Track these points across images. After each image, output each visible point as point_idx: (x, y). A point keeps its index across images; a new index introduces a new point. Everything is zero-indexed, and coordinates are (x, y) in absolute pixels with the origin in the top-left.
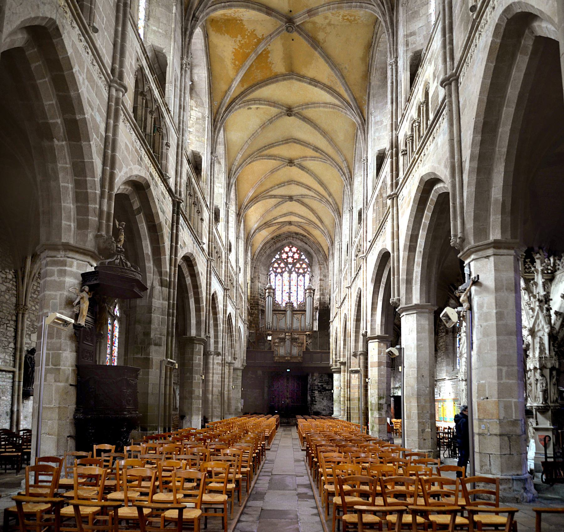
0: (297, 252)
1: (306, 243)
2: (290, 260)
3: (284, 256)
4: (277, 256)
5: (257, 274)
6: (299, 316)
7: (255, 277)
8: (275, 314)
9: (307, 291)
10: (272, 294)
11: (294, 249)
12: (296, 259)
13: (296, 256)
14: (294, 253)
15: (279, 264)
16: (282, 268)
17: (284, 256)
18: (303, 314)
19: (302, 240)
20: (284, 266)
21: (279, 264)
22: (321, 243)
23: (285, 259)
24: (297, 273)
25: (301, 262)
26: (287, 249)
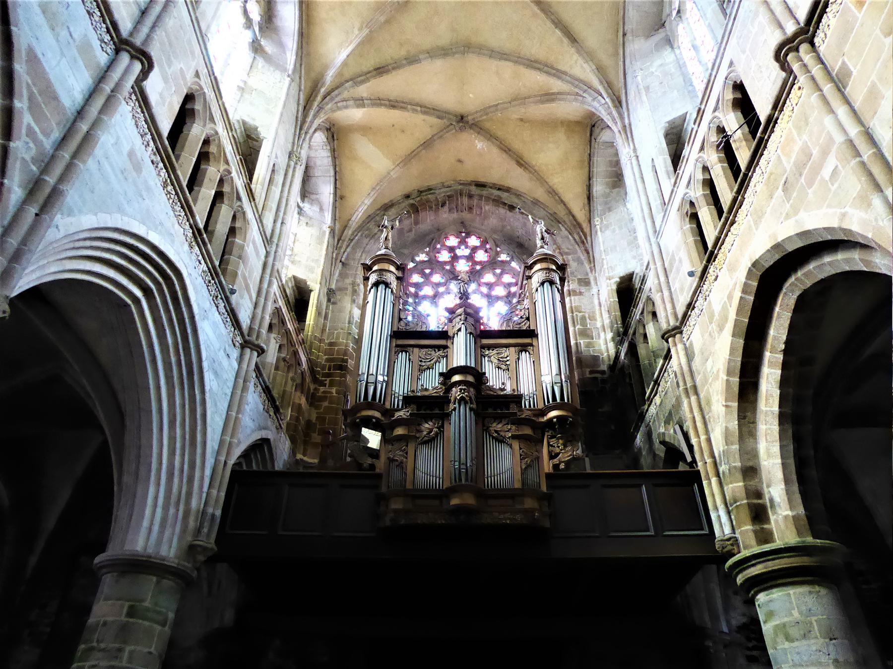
0: (483, 246)
1: (512, 208)
2: (462, 266)
3: (444, 256)
4: (422, 257)
5: (349, 281)
6: (510, 354)
7: (340, 289)
8: (403, 348)
9: (538, 267)
10: (391, 279)
11: (473, 241)
12: (480, 263)
13: (481, 256)
14: (474, 249)
15: (426, 277)
16: (438, 285)
17: (444, 256)
18: (524, 348)
19: (498, 202)
20: (443, 281)
21: (426, 277)
22: (560, 191)
23: (446, 263)
24: (488, 296)
25: (498, 271)
26: (452, 241)
